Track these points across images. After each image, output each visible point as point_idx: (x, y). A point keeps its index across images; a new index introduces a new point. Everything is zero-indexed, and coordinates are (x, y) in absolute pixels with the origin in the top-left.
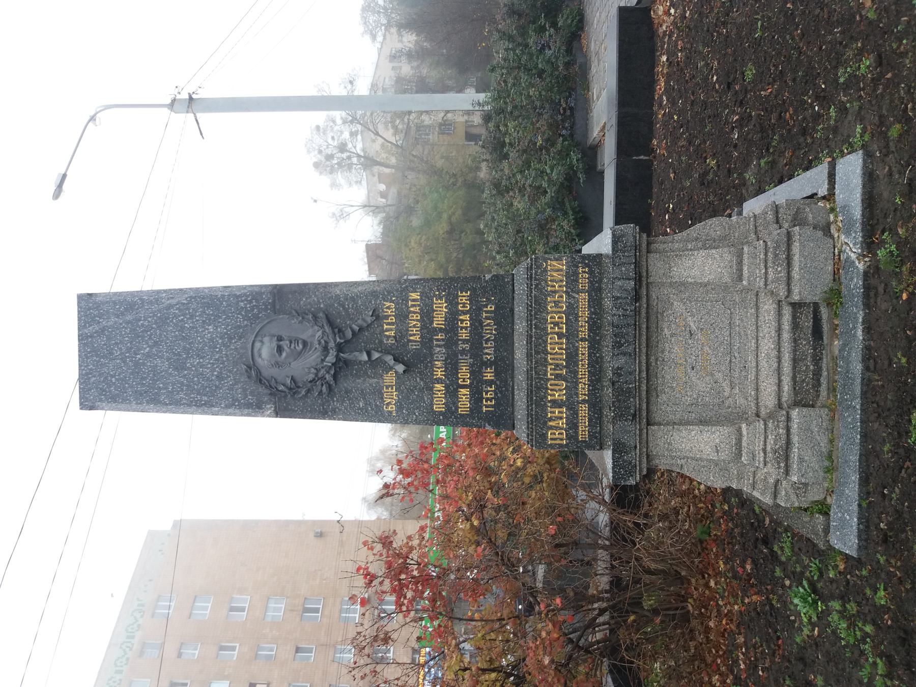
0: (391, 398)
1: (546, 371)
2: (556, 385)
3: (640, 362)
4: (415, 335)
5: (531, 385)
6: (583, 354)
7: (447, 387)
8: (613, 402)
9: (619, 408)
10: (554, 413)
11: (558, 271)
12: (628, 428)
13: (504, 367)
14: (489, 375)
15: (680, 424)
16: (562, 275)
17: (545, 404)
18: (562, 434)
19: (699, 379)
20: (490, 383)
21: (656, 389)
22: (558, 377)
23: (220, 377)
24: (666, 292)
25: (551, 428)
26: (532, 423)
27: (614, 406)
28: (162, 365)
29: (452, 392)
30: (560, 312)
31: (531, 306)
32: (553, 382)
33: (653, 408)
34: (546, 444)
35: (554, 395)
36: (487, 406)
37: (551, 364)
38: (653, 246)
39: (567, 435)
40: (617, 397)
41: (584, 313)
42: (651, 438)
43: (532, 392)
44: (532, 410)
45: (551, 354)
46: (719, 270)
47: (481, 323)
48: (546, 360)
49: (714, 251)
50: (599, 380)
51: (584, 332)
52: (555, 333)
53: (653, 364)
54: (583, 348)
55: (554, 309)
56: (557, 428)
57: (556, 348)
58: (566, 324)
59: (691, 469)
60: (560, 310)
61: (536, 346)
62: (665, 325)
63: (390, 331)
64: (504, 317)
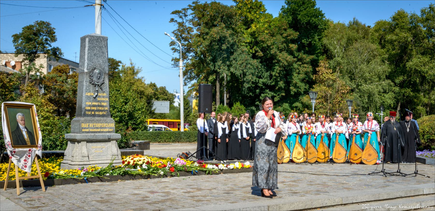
13: (94, 115)
14: (93, 113)
23: (93, 62)
28: (95, 52)
29: (90, 106)
36: (87, 113)
41: (105, 130)
51: (102, 130)
54: (99, 130)
57: (99, 125)
64: (103, 116)
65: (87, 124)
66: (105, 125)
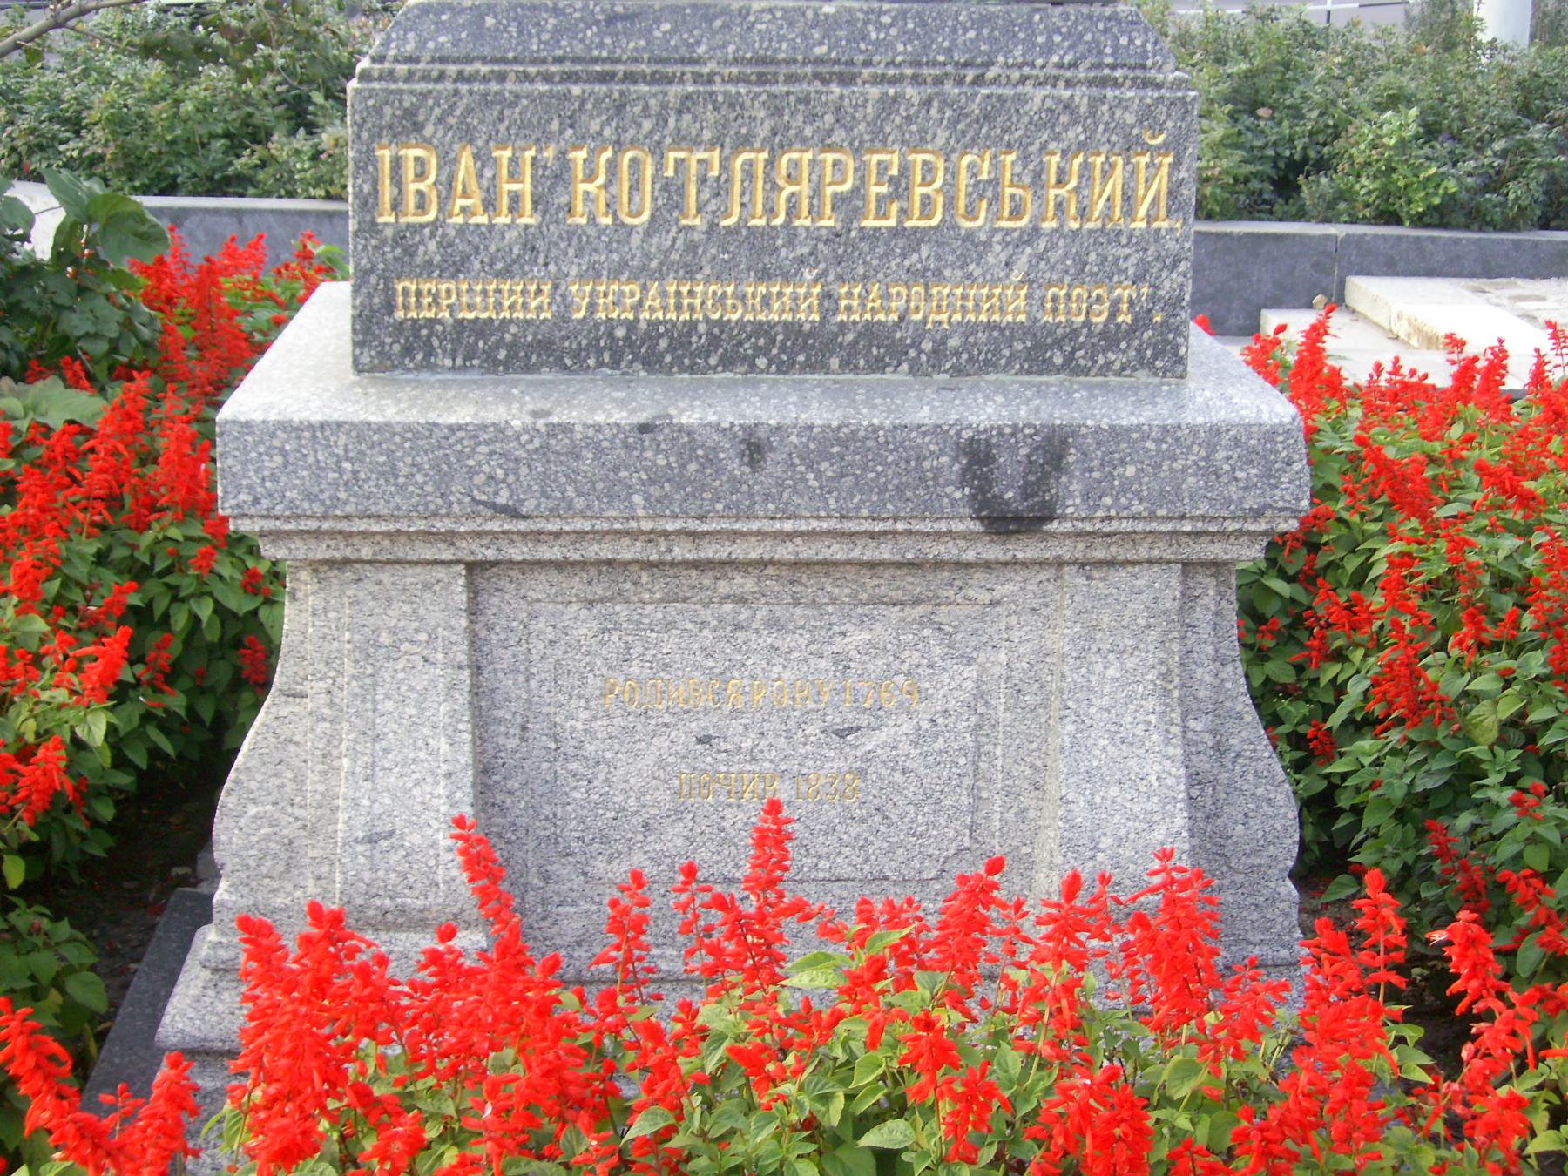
1: (696, 143)
2: (635, 187)
3: (735, 535)
5: (630, 78)
6: (766, 301)
8: (567, 429)
9: (545, 449)
10: (513, 176)
11: (1128, 198)
12: (457, 488)
15: (476, 692)
16: (1107, 216)
17: (549, 136)
18: (422, 207)
19: (661, 763)
21: (620, 596)
22: (671, 192)
24: (1016, 636)
25: (448, 162)
26: (460, 77)
27: (554, 430)
30: (950, 204)
31: (979, 81)
32: (649, 172)
33: (539, 586)
34: (376, 135)
35: (590, 178)
37: (725, 166)
38: (1208, 586)
39: (416, 229)
40: (590, 443)
41: (941, 306)
42: (413, 576)
43: (604, 78)
44: (526, 78)
45: (771, 163)
46: (1106, 842)
48: (744, 142)
49: (1181, 820)
50: (652, 362)
51: (861, 304)
52: (862, 180)
53: (723, 588)
54: (794, 302)
55: (964, 179)
56: (447, 187)
57: (804, 183)
58: (896, 232)
59: (285, 732)
60: (962, 203)
61: (805, 100)
62: (882, 633)
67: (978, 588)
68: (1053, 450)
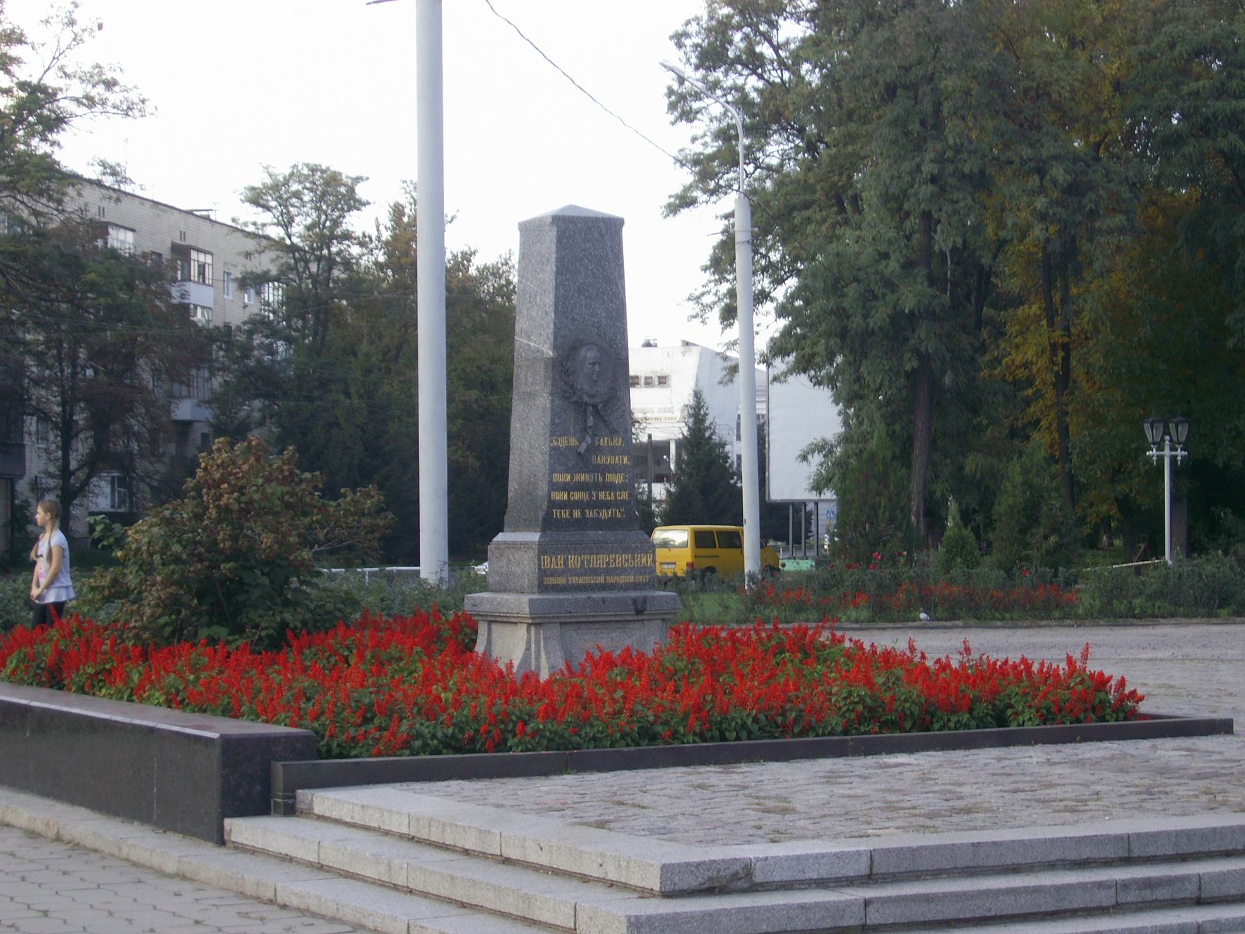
0: (562, 442)
4: (601, 460)
7: (568, 483)
13: (582, 524)
14: (577, 514)
20: (571, 514)
22: (582, 562)
23: (573, 319)
29: (566, 487)
36: (557, 513)
41: (621, 579)
47: (608, 508)
51: (610, 580)
57: (600, 561)
63: (603, 442)
64: (612, 524)
65: (561, 558)
66: (620, 560)
67: (631, 625)
68: (645, 599)
